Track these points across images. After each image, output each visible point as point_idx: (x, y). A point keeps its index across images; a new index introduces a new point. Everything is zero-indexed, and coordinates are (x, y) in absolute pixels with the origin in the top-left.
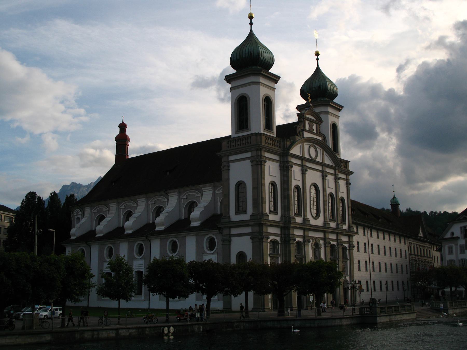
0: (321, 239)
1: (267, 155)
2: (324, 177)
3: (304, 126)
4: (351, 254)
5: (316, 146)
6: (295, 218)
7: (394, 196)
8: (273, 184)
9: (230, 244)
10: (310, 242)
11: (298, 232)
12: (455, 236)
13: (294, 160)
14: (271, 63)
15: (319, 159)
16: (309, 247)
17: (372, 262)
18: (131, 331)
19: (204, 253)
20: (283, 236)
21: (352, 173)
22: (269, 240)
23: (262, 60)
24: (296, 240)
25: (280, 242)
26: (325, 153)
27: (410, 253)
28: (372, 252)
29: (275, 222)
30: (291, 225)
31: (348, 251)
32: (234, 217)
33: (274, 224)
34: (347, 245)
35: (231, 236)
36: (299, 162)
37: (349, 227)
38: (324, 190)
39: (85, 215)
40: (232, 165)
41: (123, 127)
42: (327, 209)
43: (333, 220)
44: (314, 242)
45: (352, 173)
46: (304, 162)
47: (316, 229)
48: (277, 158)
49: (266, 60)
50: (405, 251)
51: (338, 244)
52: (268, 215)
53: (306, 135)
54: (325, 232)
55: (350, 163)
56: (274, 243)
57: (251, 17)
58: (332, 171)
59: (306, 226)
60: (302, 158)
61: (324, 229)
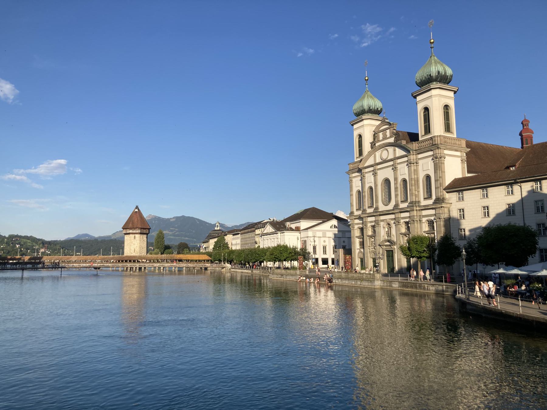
0: (392, 219)
2: (395, 169)
5: (386, 148)
13: (367, 170)
15: (391, 156)
38: (396, 179)
47: (382, 213)
59: (377, 213)
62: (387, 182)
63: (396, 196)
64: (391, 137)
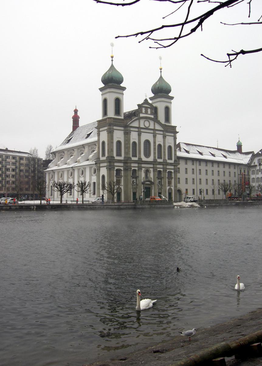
1: (115, 128)
3: (141, 111)
4: (175, 175)
5: (149, 120)
6: (131, 158)
7: (239, 141)
8: (119, 143)
9: (100, 171)
10: (142, 169)
11: (133, 165)
12: (255, 164)
13: (132, 129)
14: (121, 80)
15: (152, 127)
16: (141, 173)
17: (199, 179)
18: (16, 207)
19: (92, 175)
20: (124, 167)
21: (178, 132)
22: (115, 169)
23: (114, 80)
24: (132, 169)
25: (123, 170)
26: (156, 123)
27: (239, 173)
28: (200, 174)
29: (118, 160)
30: (128, 161)
31: (173, 174)
32: (102, 158)
33: (119, 161)
34: (173, 171)
35: (100, 167)
36: (137, 130)
37: (175, 161)
38: (155, 143)
39: (56, 157)
40: (100, 133)
41: (76, 111)
42: (156, 153)
43: (160, 157)
44: (146, 169)
45: (178, 132)
46: (139, 129)
48: (122, 128)
49: (117, 80)
50: (235, 173)
51: (163, 171)
52: (114, 157)
53: (141, 115)
54: (153, 164)
55: (176, 128)
56: (118, 171)
57: (112, 57)
58: (162, 133)
59: (140, 162)
60: (139, 128)
61: (154, 162)
62: (147, 142)
63: (155, 153)
64: (151, 114)
